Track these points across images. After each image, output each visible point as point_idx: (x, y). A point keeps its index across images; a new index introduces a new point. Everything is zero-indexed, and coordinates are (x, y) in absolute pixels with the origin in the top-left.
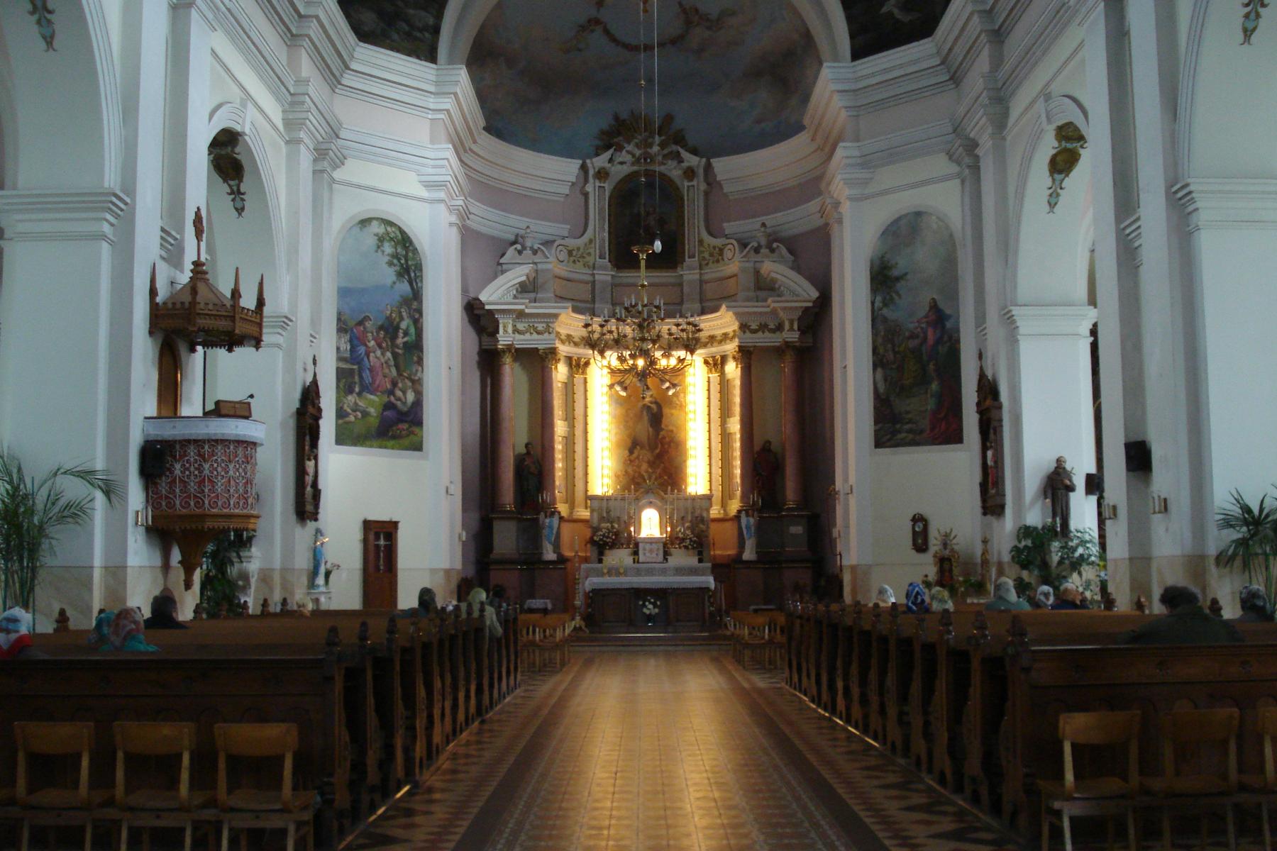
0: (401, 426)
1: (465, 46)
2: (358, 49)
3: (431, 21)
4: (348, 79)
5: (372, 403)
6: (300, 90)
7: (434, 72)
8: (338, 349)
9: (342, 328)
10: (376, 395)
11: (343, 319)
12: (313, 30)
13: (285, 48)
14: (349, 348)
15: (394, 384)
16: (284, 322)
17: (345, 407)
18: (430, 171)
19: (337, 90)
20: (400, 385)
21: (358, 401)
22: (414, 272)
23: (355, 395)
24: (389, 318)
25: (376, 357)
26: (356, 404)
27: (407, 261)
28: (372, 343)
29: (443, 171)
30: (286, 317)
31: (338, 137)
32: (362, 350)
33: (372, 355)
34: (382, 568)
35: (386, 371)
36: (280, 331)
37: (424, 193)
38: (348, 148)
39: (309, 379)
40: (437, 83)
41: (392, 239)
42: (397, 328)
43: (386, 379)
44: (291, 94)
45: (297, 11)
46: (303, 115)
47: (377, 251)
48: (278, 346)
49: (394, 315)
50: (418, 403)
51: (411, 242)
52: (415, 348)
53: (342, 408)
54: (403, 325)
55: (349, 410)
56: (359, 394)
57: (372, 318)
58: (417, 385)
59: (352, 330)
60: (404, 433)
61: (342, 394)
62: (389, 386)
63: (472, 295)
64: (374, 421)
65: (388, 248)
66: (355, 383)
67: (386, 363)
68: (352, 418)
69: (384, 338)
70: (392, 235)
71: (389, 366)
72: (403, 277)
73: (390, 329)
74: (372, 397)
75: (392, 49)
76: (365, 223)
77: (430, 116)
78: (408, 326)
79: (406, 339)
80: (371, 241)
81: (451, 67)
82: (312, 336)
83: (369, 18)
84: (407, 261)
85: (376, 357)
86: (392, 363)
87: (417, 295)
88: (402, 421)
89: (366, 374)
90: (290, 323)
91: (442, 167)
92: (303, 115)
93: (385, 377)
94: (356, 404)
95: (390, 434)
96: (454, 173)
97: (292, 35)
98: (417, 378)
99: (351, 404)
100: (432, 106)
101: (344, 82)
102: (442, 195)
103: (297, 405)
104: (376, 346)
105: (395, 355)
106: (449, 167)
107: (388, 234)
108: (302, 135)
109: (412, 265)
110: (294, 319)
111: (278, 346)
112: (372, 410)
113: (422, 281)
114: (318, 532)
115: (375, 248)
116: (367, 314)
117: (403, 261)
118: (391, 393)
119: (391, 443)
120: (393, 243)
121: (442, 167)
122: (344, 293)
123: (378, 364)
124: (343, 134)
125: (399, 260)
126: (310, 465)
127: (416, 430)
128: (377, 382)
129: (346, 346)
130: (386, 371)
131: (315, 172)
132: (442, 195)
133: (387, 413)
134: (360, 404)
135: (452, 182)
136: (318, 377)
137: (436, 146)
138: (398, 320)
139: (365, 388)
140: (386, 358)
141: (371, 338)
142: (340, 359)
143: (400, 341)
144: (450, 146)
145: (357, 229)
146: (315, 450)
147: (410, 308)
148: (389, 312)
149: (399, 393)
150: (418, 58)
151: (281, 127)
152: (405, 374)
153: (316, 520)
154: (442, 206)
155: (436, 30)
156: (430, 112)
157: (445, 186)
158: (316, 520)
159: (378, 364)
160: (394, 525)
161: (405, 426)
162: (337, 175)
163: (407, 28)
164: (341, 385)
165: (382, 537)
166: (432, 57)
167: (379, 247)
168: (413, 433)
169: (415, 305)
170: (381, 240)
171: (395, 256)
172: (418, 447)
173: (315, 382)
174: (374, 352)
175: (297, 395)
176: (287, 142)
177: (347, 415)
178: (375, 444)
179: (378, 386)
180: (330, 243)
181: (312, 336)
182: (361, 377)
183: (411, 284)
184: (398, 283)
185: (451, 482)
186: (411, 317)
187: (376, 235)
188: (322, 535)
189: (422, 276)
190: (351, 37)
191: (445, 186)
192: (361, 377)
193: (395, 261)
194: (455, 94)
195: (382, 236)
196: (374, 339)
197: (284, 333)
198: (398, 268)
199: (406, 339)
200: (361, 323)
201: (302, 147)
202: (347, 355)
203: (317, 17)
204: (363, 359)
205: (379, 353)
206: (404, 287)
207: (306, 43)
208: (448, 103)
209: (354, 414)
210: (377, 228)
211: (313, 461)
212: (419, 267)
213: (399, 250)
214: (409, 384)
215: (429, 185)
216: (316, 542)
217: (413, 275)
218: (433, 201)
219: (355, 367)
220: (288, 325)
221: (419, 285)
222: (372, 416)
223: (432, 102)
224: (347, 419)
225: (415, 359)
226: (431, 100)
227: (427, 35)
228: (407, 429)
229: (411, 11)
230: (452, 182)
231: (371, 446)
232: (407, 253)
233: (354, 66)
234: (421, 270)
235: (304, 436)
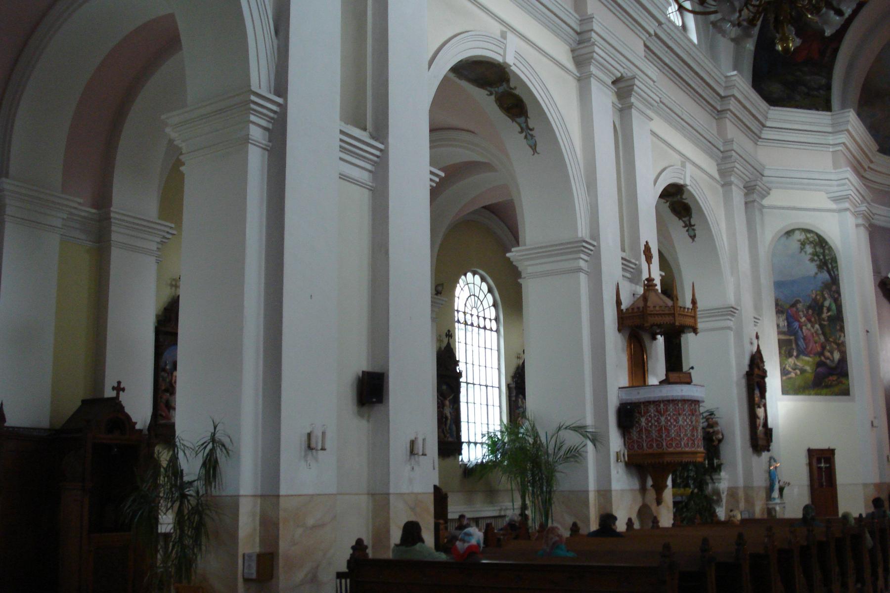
0: (831, 378)
1: (855, 93)
2: (771, 112)
3: (823, 81)
4: (766, 134)
5: (807, 363)
7: (830, 118)
8: (778, 326)
9: (780, 309)
10: (810, 357)
11: (780, 304)
13: (714, 120)
14: (786, 324)
15: (823, 348)
17: (787, 367)
18: (836, 189)
19: (758, 143)
20: (828, 348)
21: (796, 362)
22: (831, 264)
23: (793, 357)
24: (815, 300)
25: (808, 329)
26: (795, 364)
28: (803, 319)
29: (846, 187)
31: (763, 176)
32: (796, 324)
33: (804, 328)
34: (824, 484)
35: (816, 338)
37: (833, 206)
38: (771, 182)
40: (833, 125)
41: (811, 242)
42: (822, 306)
43: (817, 345)
47: (801, 252)
49: (818, 297)
50: (843, 360)
51: (826, 243)
52: (838, 319)
53: (784, 368)
54: (827, 304)
55: (790, 369)
56: (797, 357)
57: (801, 300)
58: (841, 347)
59: (787, 312)
60: (834, 383)
61: (784, 358)
62: (819, 349)
64: (810, 375)
65: (809, 249)
66: (793, 349)
67: (816, 332)
68: (793, 375)
69: (813, 314)
70: (811, 239)
71: (817, 334)
72: (823, 268)
73: (816, 307)
74: (807, 358)
75: (797, 107)
76: (789, 233)
77: (831, 150)
78: (830, 304)
79: (829, 314)
80: (797, 245)
81: (842, 111)
83: (776, 88)
85: (808, 329)
86: (820, 332)
87: (834, 281)
88: (832, 374)
89: (801, 343)
91: (844, 185)
93: (816, 343)
94: (795, 364)
95: (823, 384)
96: (854, 187)
98: (840, 342)
99: (791, 365)
100: (831, 142)
101: (763, 136)
102: (847, 205)
104: (806, 321)
105: (821, 326)
106: (850, 184)
107: (807, 238)
109: (829, 259)
112: (808, 368)
113: (837, 270)
115: (799, 250)
116: (798, 299)
117: (821, 257)
118: (821, 354)
119: (824, 391)
120: (813, 245)
121: (844, 185)
122: (779, 285)
123: (809, 334)
124: (766, 173)
125: (818, 256)
127: (844, 380)
128: (810, 348)
129: (783, 323)
130: (816, 338)
132: (847, 205)
133: (820, 369)
134: (798, 364)
135: (853, 194)
137: (837, 171)
138: (821, 300)
139: (801, 352)
140: (815, 328)
141: (802, 316)
142: (779, 333)
143: (825, 315)
144: (849, 169)
145: (784, 239)
147: (830, 290)
148: (814, 296)
149: (828, 354)
150: (817, 109)
152: (831, 339)
154: (848, 213)
155: (828, 88)
156: (831, 147)
157: (848, 198)
159: (809, 334)
160: (831, 452)
161: (835, 378)
162: (765, 202)
163: (806, 90)
164: (783, 352)
165: (823, 461)
166: (827, 107)
167: (802, 249)
168: (841, 382)
169: (834, 288)
170: (803, 244)
171: (815, 254)
172: (846, 392)
174: (806, 325)
177: (789, 373)
178: (812, 392)
179: (811, 350)
180: (764, 249)
182: (797, 345)
183: (829, 272)
184: (819, 274)
186: (832, 297)
187: (799, 241)
189: (837, 267)
190: (763, 104)
191: (848, 198)
192: (797, 345)
193: (816, 258)
194: (848, 131)
195: (804, 241)
196: (805, 316)
198: (818, 263)
199: (829, 314)
200: (794, 305)
202: (786, 329)
204: (797, 331)
205: (809, 326)
206: (825, 276)
208: (843, 138)
209: (795, 371)
210: (799, 236)
212: (834, 260)
213: (818, 249)
214: (835, 346)
215: (836, 200)
217: (830, 266)
218: (840, 211)
219: (792, 338)
221: (836, 273)
222: (809, 372)
223: (831, 139)
224: (789, 376)
225: (838, 328)
226: (831, 138)
227: (821, 92)
228: (836, 380)
229: (808, 78)
230: (853, 194)
231: (809, 394)
232: (824, 252)
233: (768, 124)
234: (836, 262)
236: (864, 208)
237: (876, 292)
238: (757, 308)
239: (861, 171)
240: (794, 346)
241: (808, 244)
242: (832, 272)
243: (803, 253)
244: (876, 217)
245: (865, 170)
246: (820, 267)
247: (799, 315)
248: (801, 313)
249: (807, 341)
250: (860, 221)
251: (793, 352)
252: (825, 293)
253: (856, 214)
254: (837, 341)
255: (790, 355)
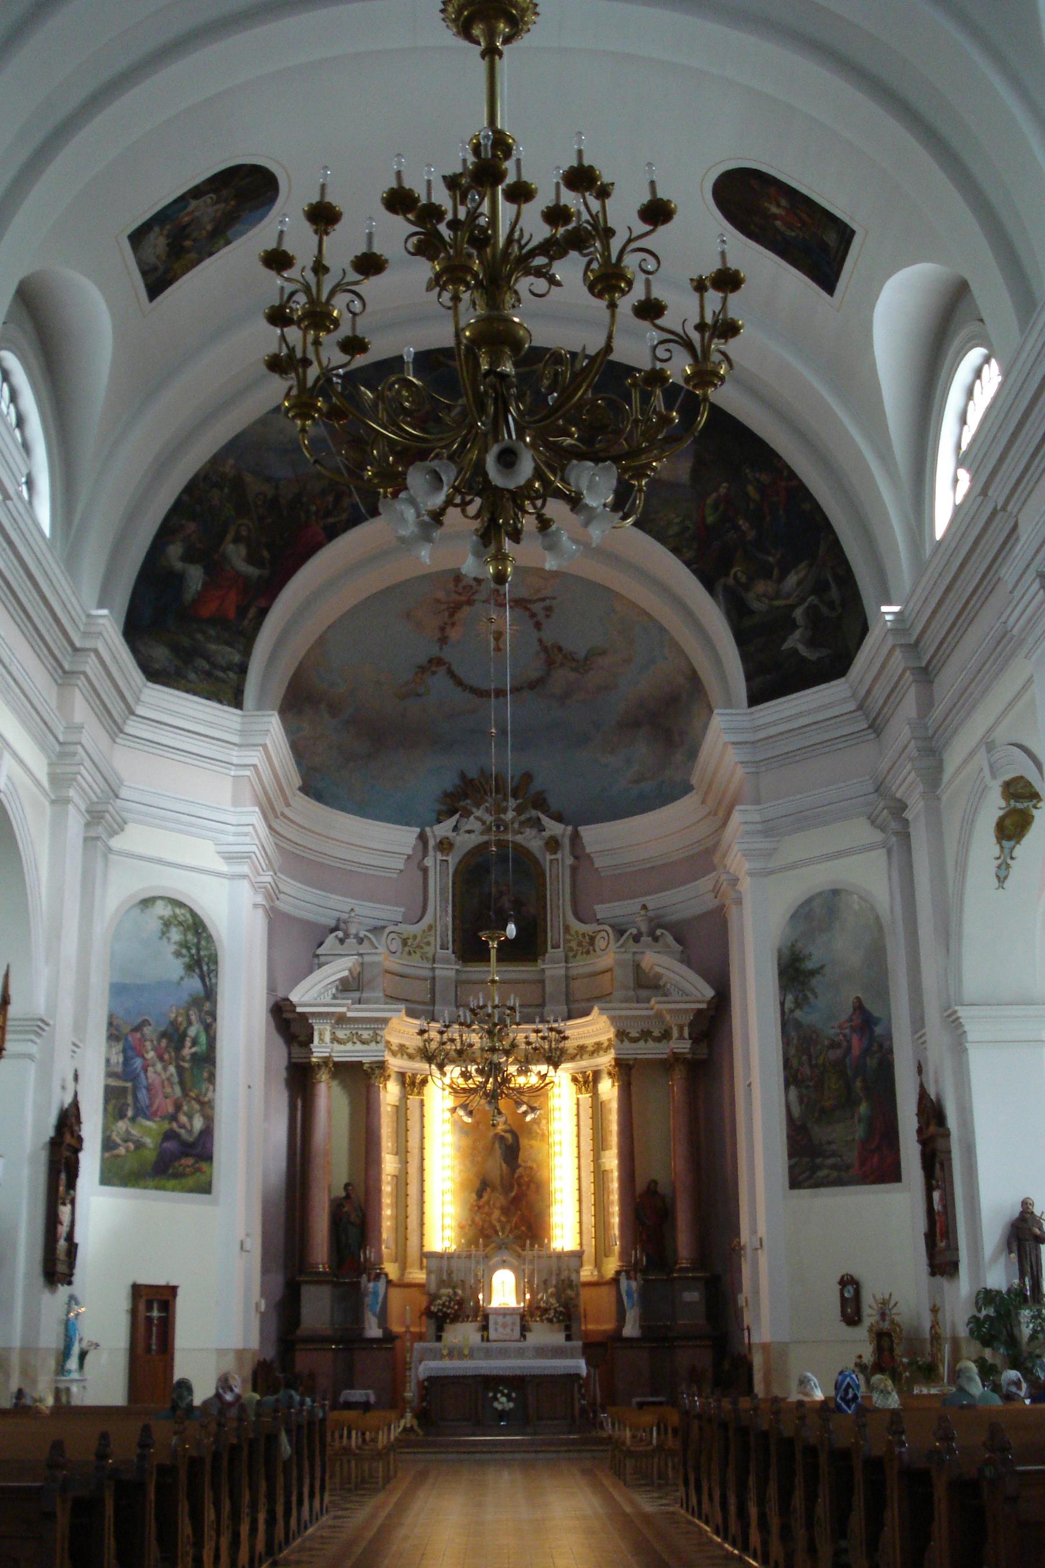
0: (183, 1161)
3: (237, 658)
6: (72, 738)
7: (239, 719)
8: (108, 1061)
9: (114, 1034)
10: (154, 1121)
12: (91, 666)
14: (121, 1059)
15: (178, 1107)
16: (38, 1026)
18: (231, 839)
20: (185, 1108)
22: (207, 964)
23: (126, 1120)
24: (174, 1023)
25: (155, 1072)
26: (128, 1132)
27: (198, 950)
28: (151, 1055)
30: (43, 1021)
32: (138, 1062)
33: (150, 1069)
35: (168, 1090)
36: (33, 1037)
37: (223, 867)
39: (68, 1100)
40: (242, 733)
41: (180, 923)
42: (184, 1036)
43: (168, 1100)
44: (60, 744)
45: (71, 643)
46: (74, 769)
47: (161, 938)
48: (30, 1057)
49: (180, 1019)
50: (207, 1132)
51: (205, 928)
52: (207, 1060)
54: (192, 1032)
55: (119, 1141)
56: (133, 1120)
57: (151, 1022)
58: (207, 1108)
59: (126, 1039)
60: (188, 1169)
61: (111, 1119)
62: (171, 1109)
63: (281, 994)
64: (150, 1155)
65: (176, 935)
66: (128, 1105)
67: (168, 1079)
68: (122, 1151)
69: (167, 1047)
70: (181, 919)
71: (171, 1084)
72: (194, 971)
74: (149, 1123)
76: (147, 902)
77: (233, 773)
78: (198, 1033)
79: (194, 1050)
80: (156, 925)
82: (75, 1044)
84: (198, 950)
85: (155, 1072)
86: (176, 1079)
87: (210, 994)
88: (187, 1155)
89: (142, 1094)
90: (46, 1028)
91: (246, 834)
92: (74, 769)
93: (166, 1097)
94: (128, 1132)
95: (170, 1171)
97: (65, 672)
98: (206, 1099)
100: (235, 761)
102: (245, 869)
103: (51, 1133)
105: (180, 1070)
107: (175, 916)
108: (72, 793)
109: (205, 956)
110: (51, 1023)
111: (30, 1057)
112: (148, 1141)
113: (216, 976)
114: (72, 1299)
115: (160, 934)
116: (146, 1018)
117: (193, 951)
118: (174, 1118)
119: (172, 1183)
120: (181, 928)
121: (246, 834)
122: (118, 990)
123: (157, 1082)
125: (188, 949)
126: (65, 1211)
127: (204, 1165)
129: (118, 1059)
130: (168, 1090)
131: (86, 839)
132: (245, 869)
133: (168, 1145)
134: (134, 1132)
136: (80, 1098)
137: (239, 809)
138: (185, 1025)
139: (141, 1112)
141: (149, 1048)
142: (110, 1074)
143: (187, 1052)
144: (257, 809)
145: (137, 911)
146: (72, 1192)
147: (200, 1011)
148: (173, 1015)
150: (220, 702)
151: (45, 782)
152: (192, 1094)
153: (70, 1283)
154: (245, 883)
155: (243, 670)
156: (233, 768)
158: (70, 1283)
159: (157, 1082)
161: (190, 1161)
163: (207, 667)
164: (110, 1108)
166: (237, 701)
167: (163, 933)
168: (200, 1170)
169: (207, 1006)
170: (167, 924)
171: (185, 945)
172: (206, 1188)
173: (75, 1104)
174: (153, 1066)
175: (52, 1119)
176: (53, 802)
177: (116, 1146)
178: (151, 1184)
179: (157, 1110)
181: (75, 1044)
182: (136, 1099)
183: (202, 978)
184: (186, 980)
185: (248, 1235)
186: (202, 1021)
187: (161, 918)
188: (77, 1303)
189: (216, 971)
192: (136, 1099)
193: (184, 951)
194: (265, 746)
195: (169, 920)
196: (154, 1049)
197: (38, 1041)
198: (187, 960)
199: (194, 1050)
200: (138, 1028)
201: (71, 808)
203: (96, 652)
204: (138, 1075)
205: (159, 1066)
206: (194, 984)
207: (81, 681)
208: (255, 757)
209: (126, 1145)
210: (162, 910)
211: (69, 1207)
212: (214, 959)
214: (197, 1107)
215: (229, 857)
216: (68, 1312)
217: (205, 968)
218: (233, 877)
219: (129, 1085)
220: (43, 1030)
221: (213, 981)
223: (235, 756)
224: (116, 1152)
225: (206, 1075)
226: (235, 753)
227: (231, 675)
228: (193, 1165)
231: (146, 1188)
232: (199, 942)
234: (216, 963)
235: (59, 1172)
236: (269, 879)
237: (268, 1024)
238: (79, 1027)
239: (271, 817)
240: (130, 1100)
241: (175, 926)
242: (207, 980)
243: (165, 940)
244: (281, 896)
245: (276, 817)
246: (189, 968)
247: (144, 1046)
248: (148, 1044)
249: (153, 1092)
250: (260, 899)
251: (127, 1109)
252: (191, 1012)
253: (255, 887)
254: (202, 1098)
255: (122, 1115)
